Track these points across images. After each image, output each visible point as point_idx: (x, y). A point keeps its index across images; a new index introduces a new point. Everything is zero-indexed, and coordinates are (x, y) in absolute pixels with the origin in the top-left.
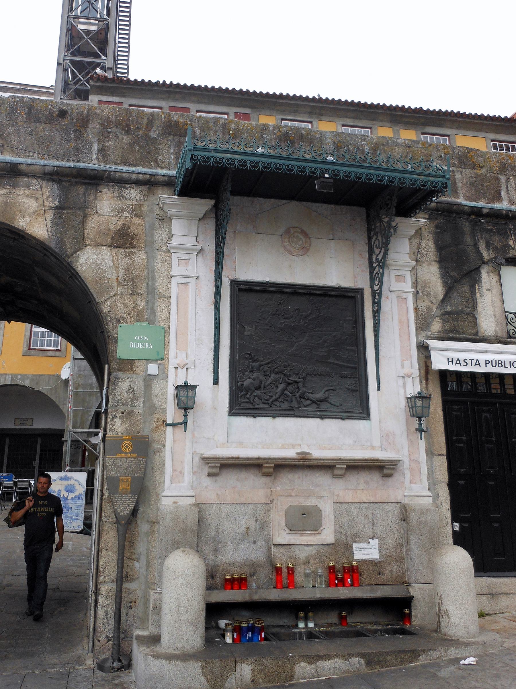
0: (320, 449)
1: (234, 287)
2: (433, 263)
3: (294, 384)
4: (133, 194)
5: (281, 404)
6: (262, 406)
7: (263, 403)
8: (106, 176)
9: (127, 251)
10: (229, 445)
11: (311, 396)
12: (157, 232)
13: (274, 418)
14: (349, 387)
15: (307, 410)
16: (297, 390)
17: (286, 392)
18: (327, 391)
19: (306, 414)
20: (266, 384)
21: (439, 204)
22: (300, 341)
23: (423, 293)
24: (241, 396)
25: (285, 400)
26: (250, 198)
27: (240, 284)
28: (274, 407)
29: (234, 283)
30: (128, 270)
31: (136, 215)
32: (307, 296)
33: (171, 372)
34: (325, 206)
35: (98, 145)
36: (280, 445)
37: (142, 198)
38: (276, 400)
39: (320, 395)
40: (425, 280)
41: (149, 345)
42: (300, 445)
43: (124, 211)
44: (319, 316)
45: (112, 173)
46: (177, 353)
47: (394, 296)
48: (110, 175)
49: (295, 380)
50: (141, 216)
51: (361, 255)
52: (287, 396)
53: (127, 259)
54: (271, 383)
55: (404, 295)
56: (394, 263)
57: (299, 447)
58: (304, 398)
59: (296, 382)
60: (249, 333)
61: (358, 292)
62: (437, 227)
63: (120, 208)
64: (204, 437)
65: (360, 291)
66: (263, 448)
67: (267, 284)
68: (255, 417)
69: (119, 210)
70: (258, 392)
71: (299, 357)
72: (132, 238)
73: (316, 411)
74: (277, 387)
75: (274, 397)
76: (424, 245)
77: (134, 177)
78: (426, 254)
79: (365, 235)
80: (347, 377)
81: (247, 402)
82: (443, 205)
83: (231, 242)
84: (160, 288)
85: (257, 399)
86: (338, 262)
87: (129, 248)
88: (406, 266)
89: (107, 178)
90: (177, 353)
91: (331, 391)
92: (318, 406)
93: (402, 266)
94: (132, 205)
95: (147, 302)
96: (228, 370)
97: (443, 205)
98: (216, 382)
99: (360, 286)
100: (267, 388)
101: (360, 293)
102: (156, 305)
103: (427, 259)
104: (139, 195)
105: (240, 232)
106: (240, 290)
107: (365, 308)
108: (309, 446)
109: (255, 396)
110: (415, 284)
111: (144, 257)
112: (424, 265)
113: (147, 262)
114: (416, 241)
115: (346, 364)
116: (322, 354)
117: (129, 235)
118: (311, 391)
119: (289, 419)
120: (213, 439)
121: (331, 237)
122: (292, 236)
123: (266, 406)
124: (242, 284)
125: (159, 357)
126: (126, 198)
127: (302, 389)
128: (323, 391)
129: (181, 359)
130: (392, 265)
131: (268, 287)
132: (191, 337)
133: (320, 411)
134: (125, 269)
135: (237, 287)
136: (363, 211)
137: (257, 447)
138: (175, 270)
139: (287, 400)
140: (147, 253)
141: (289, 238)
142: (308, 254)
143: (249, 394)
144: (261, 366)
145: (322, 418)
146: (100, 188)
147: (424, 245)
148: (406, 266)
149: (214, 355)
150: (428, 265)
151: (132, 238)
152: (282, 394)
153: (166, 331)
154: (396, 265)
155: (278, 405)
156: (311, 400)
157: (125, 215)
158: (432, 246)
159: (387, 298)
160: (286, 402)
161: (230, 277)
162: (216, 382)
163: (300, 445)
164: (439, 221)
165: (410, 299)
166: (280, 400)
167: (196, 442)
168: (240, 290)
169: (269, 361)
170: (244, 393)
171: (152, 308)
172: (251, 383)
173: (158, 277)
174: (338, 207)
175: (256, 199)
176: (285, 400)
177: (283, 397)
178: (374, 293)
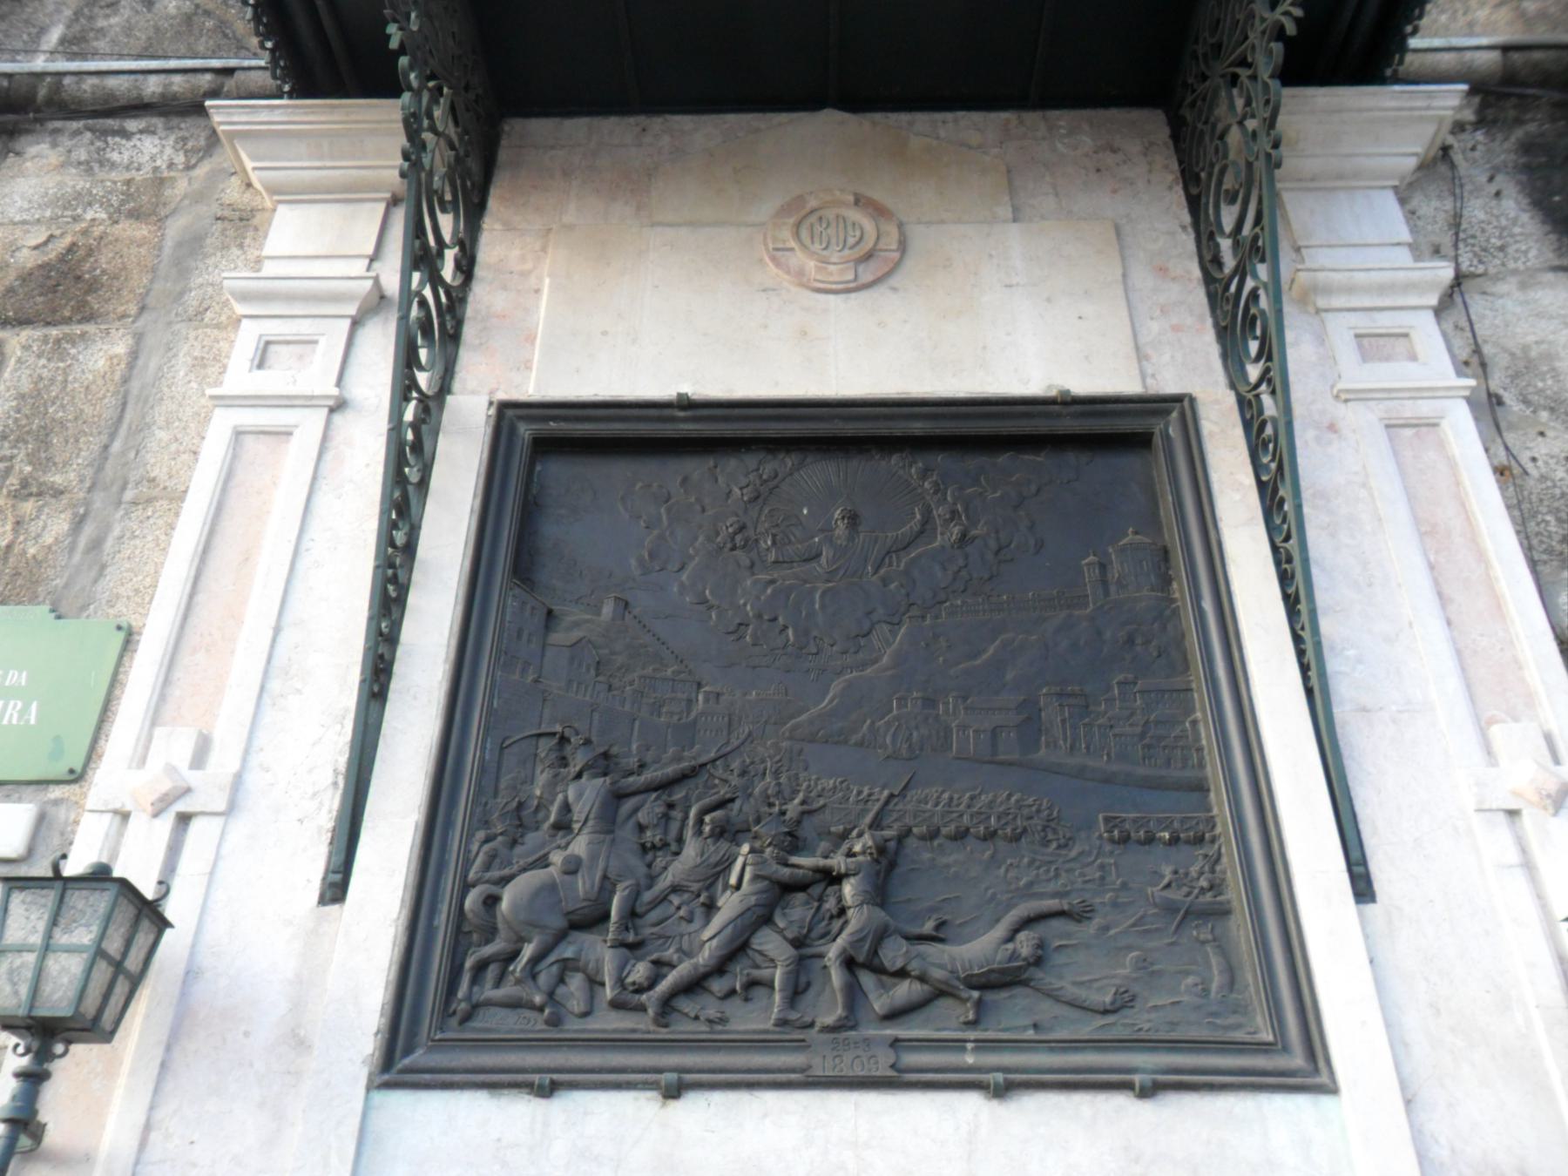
1: (513, 430)
2: (1550, 276)
3: (816, 890)
4: (148, 149)
5: (734, 1007)
8: (42, 92)
9: (54, 332)
12: (210, 261)
13: (673, 1092)
14: (1169, 894)
15: (895, 1043)
16: (837, 924)
18: (1027, 922)
19: (881, 1066)
20: (647, 896)
21: (1516, 57)
22: (863, 665)
23: (1526, 402)
24: (481, 967)
26: (632, 120)
28: (682, 1028)
29: (508, 415)
30: (33, 400)
31: (135, 215)
32: (895, 459)
34: (976, 117)
35: (68, 27)
37: (180, 159)
38: (694, 986)
39: (980, 948)
40: (1526, 349)
41: (23, 712)
43: (90, 204)
44: (964, 539)
45: (67, 81)
47: (1362, 420)
48: (57, 87)
50: (154, 213)
51: (1162, 271)
53: (43, 361)
54: (675, 889)
55: (1425, 408)
56: (1337, 277)
58: (879, 970)
60: (576, 634)
61: (1168, 412)
62: (1527, 148)
63: (78, 195)
65: (1180, 406)
68: (547, 1091)
69: (72, 202)
71: (860, 744)
72: (93, 286)
73: (958, 1045)
74: (711, 907)
76: (1481, 215)
77: (153, 86)
78: (1502, 248)
79: (1178, 195)
80: (1150, 840)
81: (514, 1004)
82: (1537, 55)
83: (528, 266)
84: (157, 463)
86: (1049, 300)
87: (67, 321)
88: (1408, 287)
89: (49, 102)
91: (1056, 924)
93: (1382, 289)
94: (128, 182)
95: (78, 523)
97: (1537, 55)
98: (336, 889)
99: (1168, 384)
100: (654, 916)
101: (1175, 415)
102: (116, 532)
103: (1511, 265)
104: (168, 151)
105: (570, 227)
106: (545, 446)
107: (1215, 477)
110: (1475, 361)
111: (121, 348)
112: (1502, 288)
113: (131, 366)
114: (1435, 203)
115: (1141, 771)
117: (78, 278)
118: (928, 927)
119: (770, 1098)
121: (1005, 211)
122: (813, 219)
124: (555, 418)
125: (59, 770)
126: (113, 165)
128: (1000, 931)
130: (1328, 290)
131: (685, 420)
133: (983, 1045)
134: (22, 397)
135: (525, 431)
136: (1155, 123)
138: (239, 377)
140: (139, 337)
141: (798, 225)
142: (894, 281)
144: (619, 796)
146: (22, 142)
147: (1481, 215)
148: (1408, 287)
150: (1523, 286)
151: (93, 286)
152: (737, 949)
153: (129, 639)
154: (1350, 289)
155: (712, 1012)
157: (89, 215)
158: (1525, 217)
159: (1332, 428)
162: (336, 889)
164: (1532, 128)
165: (1461, 430)
169: (671, 770)
171: (96, 545)
173: (161, 420)
174: (1031, 117)
175: (656, 123)
178: (1248, 409)
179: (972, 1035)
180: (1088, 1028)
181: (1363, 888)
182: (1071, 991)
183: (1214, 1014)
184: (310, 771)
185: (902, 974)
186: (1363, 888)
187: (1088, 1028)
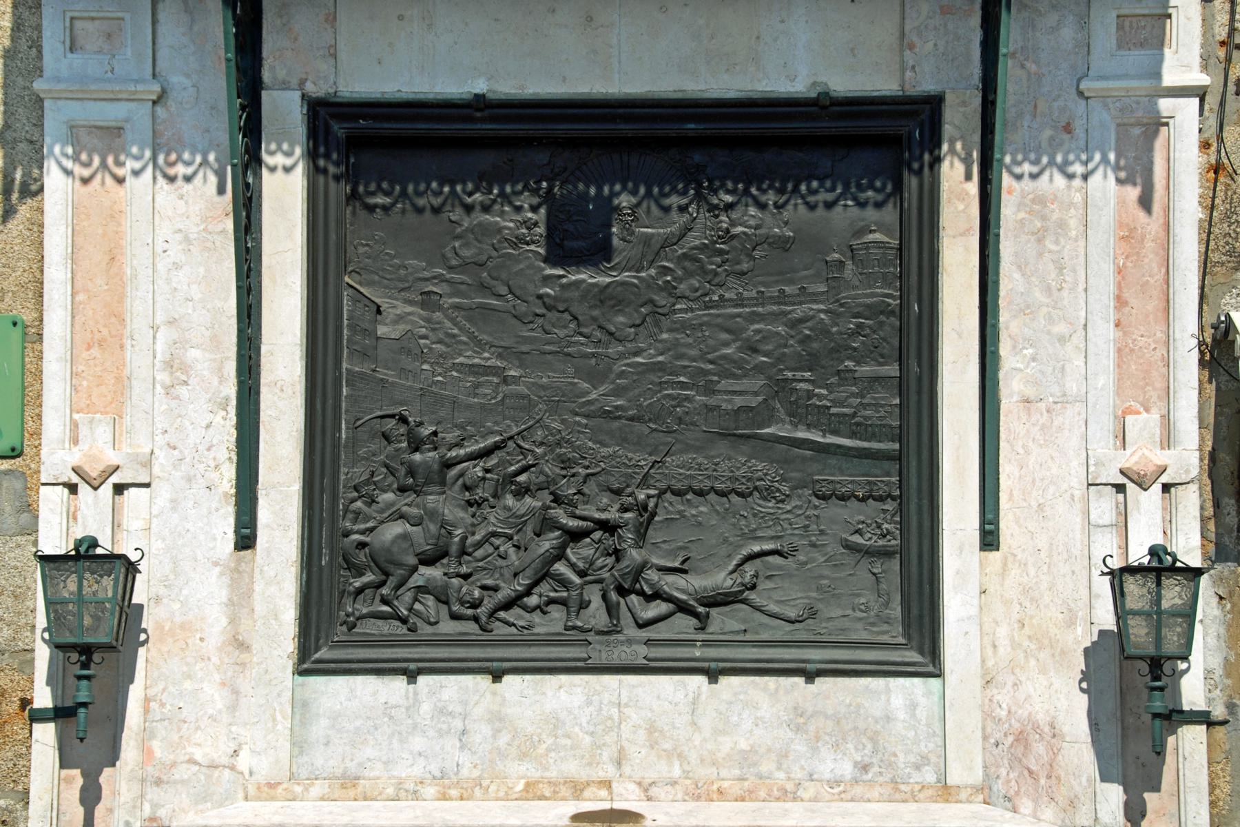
0: (698, 798)
3: (597, 535)
5: (537, 617)
6: (448, 627)
7: (455, 617)
10: (298, 789)
11: (674, 585)
17: (560, 567)
24: (360, 591)
25: (552, 601)
27: (355, 118)
33: (51, 501)
36: (520, 787)
42: (607, 784)
46: (75, 425)
49: (603, 516)
52: (564, 583)
57: (604, 793)
59: (608, 527)
64: (192, 761)
66: (444, 797)
67: (480, 103)
70: (432, 573)
73: (691, 643)
75: (505, 593)
85: (430, 600)
90: (75, 425)
92: (703, 620)
96: (295, 488)
100: (479, 553)
106: (356, 143)
108: (646, 789)
109: (420, 589)
116: (739, 401)
119: (564, 678)
120: (232, 768)
123: (471, 627)
127: (635, 555)
129: (99, 447)
131: (483, 120)
132: (138, 360)
135: (339, 130)
137: (416, 795)
139: (563, 602)
143: (392, 581)
145: (713, 676)
149: (240, 426)
156: (669, 599)
160: (557, 612)
161: (310, 88)
163: (607, 784)
166: (533, 600)
167: (158, 782)
168: (356, 143)
170: (369, 577)
172: (405, 536)
176: (552, 601)
177: (544, 588)
179: (701, 637)
180: (782, 631)
181: (989, 539)
182: (773, 608)
183: (873, 624)
184: (209, 449)
185: (657, 595)
186: (989, 539)
187: (782, 631)
